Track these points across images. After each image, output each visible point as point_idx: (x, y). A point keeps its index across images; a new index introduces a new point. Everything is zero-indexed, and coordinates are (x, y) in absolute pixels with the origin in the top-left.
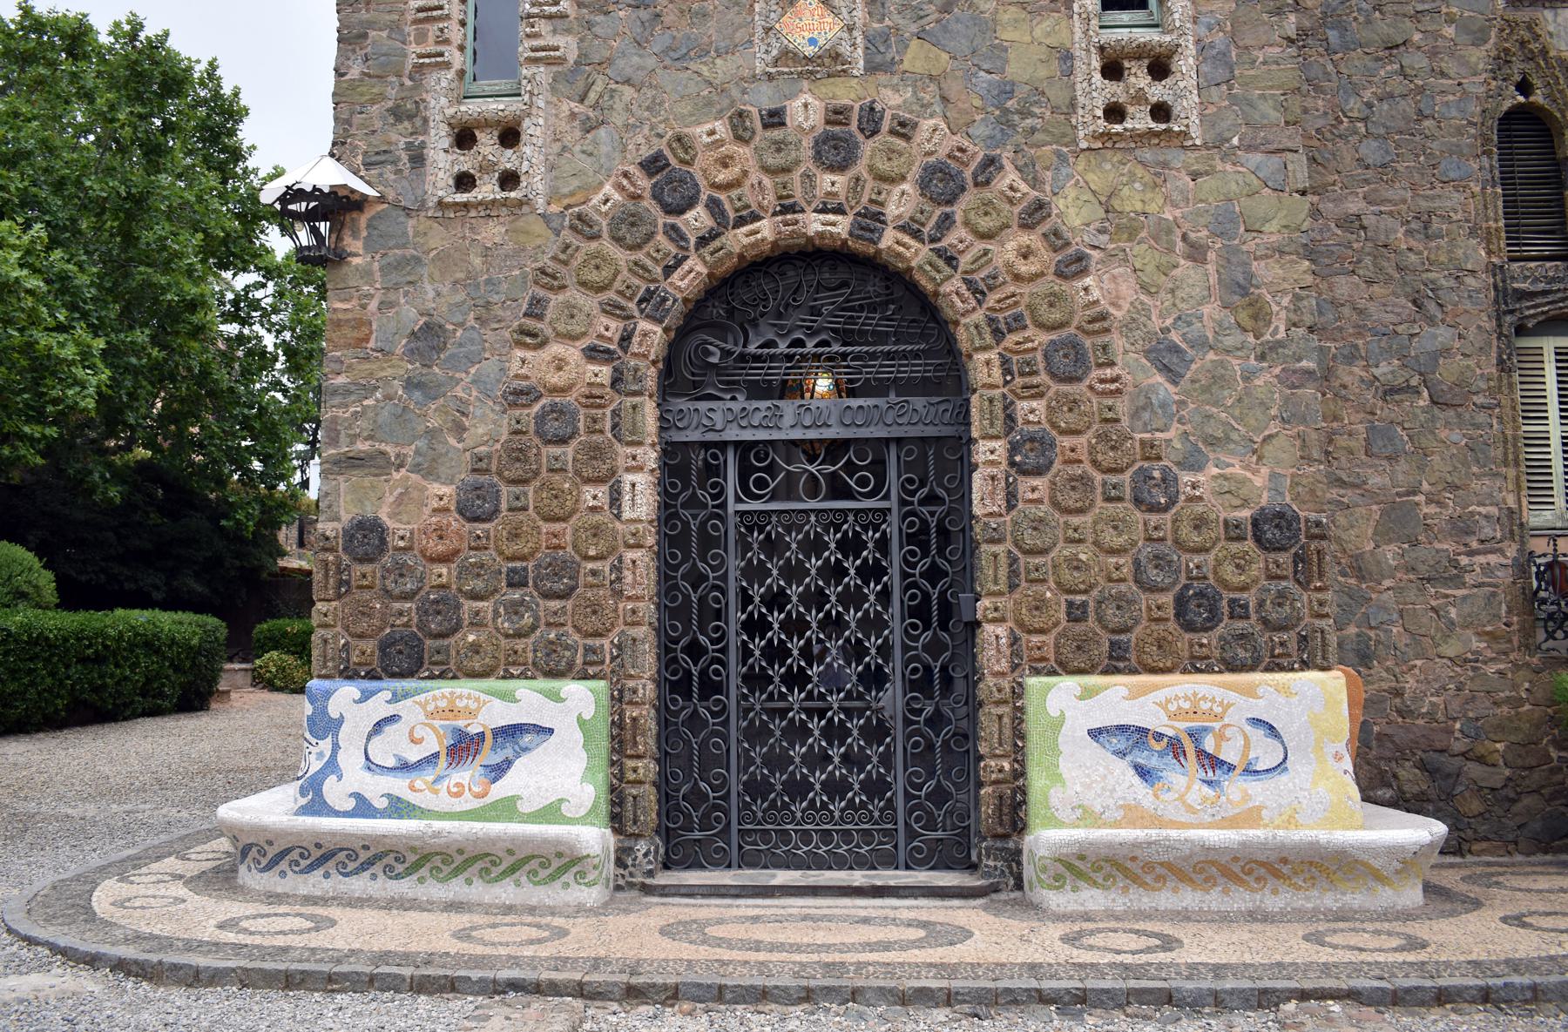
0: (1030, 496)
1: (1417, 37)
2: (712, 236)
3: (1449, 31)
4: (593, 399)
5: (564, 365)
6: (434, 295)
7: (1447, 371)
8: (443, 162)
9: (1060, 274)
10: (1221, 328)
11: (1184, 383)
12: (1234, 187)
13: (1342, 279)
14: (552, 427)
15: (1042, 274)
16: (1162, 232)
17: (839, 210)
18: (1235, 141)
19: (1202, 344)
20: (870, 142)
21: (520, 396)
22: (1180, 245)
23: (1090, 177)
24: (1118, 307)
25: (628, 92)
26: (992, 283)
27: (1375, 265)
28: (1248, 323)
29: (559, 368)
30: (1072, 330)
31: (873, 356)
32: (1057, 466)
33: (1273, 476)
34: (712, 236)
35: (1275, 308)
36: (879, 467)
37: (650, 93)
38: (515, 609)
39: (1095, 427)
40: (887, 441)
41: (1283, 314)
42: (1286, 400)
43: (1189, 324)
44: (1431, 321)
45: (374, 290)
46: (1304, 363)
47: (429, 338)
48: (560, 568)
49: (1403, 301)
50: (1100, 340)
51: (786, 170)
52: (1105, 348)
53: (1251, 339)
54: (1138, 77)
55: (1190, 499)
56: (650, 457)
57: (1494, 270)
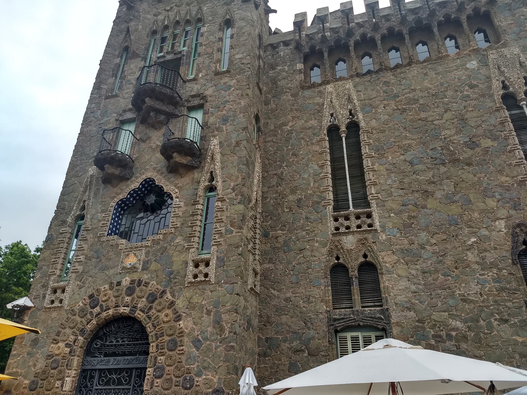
0: (156, 385)
1: (308, 247)
2: (99, 314)
3: (317, 245)
7: (313, 344)
9: (174, 321)
10: (212, 334)
11: (200, 351)
12: (220, 294)
13: (284, 317)
15: (170, 321)
16: (202, 307)
17: (127, 306)
18: (222, 282)
19: (206, 339)
20: (138, 288)
22: (205, 310)
23: (187, 294)
24: (186, 329)
25: (90, 279)
27: (293, 312)
28: (219, 332)
29: (59, 349)
30: (175, 336)
31: (137, 344)
32: (165, 376)
33: (219, 379)
34: (99, 314)
35: (226, 328)
36: (130, 377)
37: (95, 279)
39: (176, 364)
40: (133, 368)
41: (228, 330)
42: (225, 355)
43: (204, 333)
44: (309, 328)
46: (231, 344)
49: (301, 322)
50: (180, 339)
51: (118, 296)
52: (181, 341)
53: (219, 337)
54: (202, 267)
55: (197, 386)
57: (327, 312)
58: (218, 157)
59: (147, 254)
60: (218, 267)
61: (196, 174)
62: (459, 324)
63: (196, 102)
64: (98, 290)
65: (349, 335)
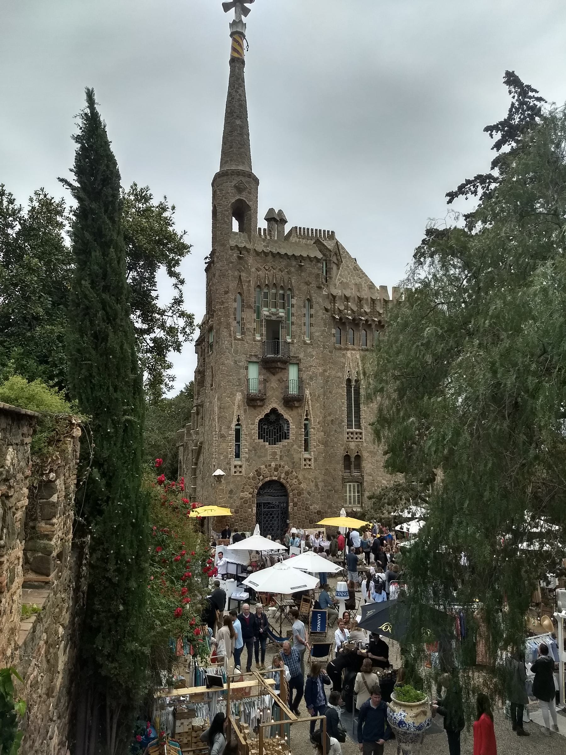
4: (250, 499)
5: (246, 495)
6: (232, 486)
8: (233, 470)
14: (245, 502)
16: (309, 479)
19: (313, 492)
21: (242, 498)
26: (292, 485)
38: (241, 524)
45: (225, 486)
47: (231, 492)
48: (247, 519)
54: (308, 462)
56: (256, 505)
58: (310, 402)
59: (281, 451)
60: (315, 462)
61: (300, 411)
62: (385, 482)
63: (295, 361)
64: (260, 468)
65: (348, 484)
